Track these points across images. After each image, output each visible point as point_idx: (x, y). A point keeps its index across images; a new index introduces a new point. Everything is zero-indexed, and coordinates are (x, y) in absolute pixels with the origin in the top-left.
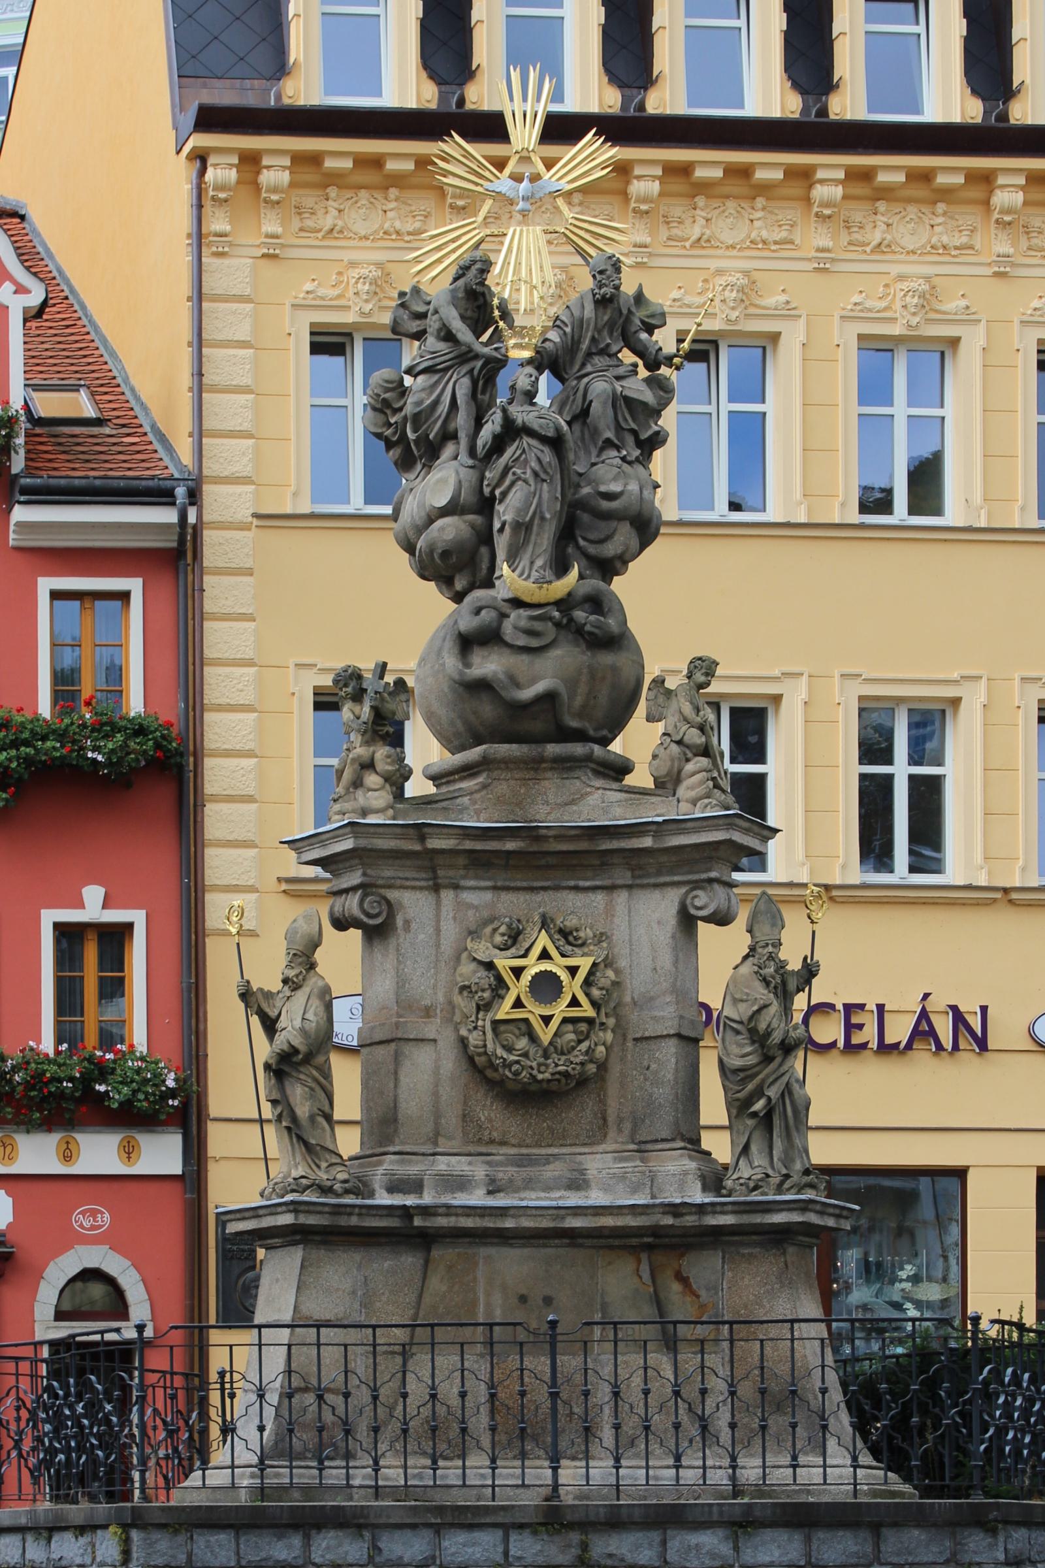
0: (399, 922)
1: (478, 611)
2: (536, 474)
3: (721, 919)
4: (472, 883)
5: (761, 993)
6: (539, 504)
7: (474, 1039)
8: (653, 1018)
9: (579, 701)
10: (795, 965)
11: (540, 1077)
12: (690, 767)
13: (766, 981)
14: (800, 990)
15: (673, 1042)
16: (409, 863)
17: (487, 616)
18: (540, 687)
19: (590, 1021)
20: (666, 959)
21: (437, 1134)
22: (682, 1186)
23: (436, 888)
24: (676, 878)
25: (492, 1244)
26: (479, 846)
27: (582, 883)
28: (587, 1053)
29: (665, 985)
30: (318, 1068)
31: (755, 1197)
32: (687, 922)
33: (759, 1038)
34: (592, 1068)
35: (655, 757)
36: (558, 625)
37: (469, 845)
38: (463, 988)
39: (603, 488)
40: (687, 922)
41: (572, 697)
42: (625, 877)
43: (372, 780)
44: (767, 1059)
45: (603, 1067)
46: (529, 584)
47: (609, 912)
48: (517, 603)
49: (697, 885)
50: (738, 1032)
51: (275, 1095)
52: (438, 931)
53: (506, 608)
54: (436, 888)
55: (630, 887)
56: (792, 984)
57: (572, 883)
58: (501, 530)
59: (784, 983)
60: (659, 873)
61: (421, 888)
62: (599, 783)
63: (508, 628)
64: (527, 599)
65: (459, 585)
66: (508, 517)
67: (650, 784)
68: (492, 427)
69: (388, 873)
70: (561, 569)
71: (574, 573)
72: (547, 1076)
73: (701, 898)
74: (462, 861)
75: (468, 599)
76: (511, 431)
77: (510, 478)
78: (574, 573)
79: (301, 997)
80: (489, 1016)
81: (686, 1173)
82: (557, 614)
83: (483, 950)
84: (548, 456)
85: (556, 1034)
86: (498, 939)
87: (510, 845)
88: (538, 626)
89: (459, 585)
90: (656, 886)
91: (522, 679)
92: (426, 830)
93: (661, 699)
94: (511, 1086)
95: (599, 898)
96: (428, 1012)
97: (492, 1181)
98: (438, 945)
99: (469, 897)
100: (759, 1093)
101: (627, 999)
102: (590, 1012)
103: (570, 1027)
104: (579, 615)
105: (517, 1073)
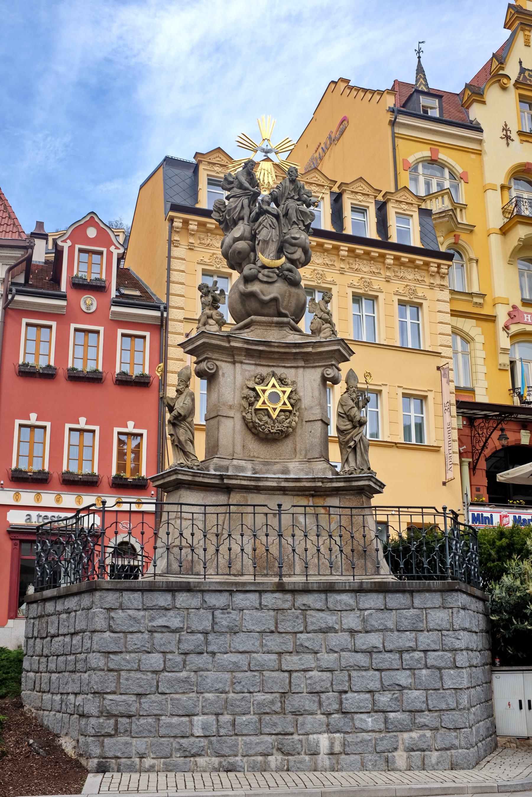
0: (220, 373)
1: (250, 269)
2: (271, 226)
6: (271, 236)
7: (248, 416)
8: (312, 414)
9: (285, 303)
11: (272, 431)
15: (320, 422)
18: (272, 296)
19: (290, 412)
20: (316, 393)
21: (234, 452)
22: (324, 473)
23: (234, 363)
24: (320, 364)
25: (254, 493)
27: (287, 365)
28: (289, 423)
29: (316, 402)
34: (290, 430)
35: (312, 323)
38: (244, 397)
39: (293, 236)
41: (283, 302)
43: (211, 321)
45: (294, 429)
46: (269, 260)
47: (296, 376)
48: (264, 267)
51: (172, 432)
52: (235, 378)
53: (260, 269)
55: (304, 367)
57: (283, 365)
58: (258, 244)
61: (229, 362)
62: (291, 332)
63: (260, 276)
64: (267, 265)
66: (261, 238)
67: (310, 333)
68: (256, 210)
70: (279, 258)
72: (274, 431)
74: (243, 353)
76: (262, 212)
77: (262, 226)
80: (253, 408)
81: (325, 468)
82: (278, 271)
83: (251, 384)
84: (274, 220)
85: (278, 416)
86: (257, 380)
87: (261, 348)
88: (271, 274)
90: (313, 367)
91: (265, 293)
93: (313, 306)
94: (261, 435)
95: (293, 371)
96: (231, 407)
97: (254, 469)
98: (235, 383)
101: (303, 407)
102: (290, 408)
103: (283, 413)
105: (263, 429)
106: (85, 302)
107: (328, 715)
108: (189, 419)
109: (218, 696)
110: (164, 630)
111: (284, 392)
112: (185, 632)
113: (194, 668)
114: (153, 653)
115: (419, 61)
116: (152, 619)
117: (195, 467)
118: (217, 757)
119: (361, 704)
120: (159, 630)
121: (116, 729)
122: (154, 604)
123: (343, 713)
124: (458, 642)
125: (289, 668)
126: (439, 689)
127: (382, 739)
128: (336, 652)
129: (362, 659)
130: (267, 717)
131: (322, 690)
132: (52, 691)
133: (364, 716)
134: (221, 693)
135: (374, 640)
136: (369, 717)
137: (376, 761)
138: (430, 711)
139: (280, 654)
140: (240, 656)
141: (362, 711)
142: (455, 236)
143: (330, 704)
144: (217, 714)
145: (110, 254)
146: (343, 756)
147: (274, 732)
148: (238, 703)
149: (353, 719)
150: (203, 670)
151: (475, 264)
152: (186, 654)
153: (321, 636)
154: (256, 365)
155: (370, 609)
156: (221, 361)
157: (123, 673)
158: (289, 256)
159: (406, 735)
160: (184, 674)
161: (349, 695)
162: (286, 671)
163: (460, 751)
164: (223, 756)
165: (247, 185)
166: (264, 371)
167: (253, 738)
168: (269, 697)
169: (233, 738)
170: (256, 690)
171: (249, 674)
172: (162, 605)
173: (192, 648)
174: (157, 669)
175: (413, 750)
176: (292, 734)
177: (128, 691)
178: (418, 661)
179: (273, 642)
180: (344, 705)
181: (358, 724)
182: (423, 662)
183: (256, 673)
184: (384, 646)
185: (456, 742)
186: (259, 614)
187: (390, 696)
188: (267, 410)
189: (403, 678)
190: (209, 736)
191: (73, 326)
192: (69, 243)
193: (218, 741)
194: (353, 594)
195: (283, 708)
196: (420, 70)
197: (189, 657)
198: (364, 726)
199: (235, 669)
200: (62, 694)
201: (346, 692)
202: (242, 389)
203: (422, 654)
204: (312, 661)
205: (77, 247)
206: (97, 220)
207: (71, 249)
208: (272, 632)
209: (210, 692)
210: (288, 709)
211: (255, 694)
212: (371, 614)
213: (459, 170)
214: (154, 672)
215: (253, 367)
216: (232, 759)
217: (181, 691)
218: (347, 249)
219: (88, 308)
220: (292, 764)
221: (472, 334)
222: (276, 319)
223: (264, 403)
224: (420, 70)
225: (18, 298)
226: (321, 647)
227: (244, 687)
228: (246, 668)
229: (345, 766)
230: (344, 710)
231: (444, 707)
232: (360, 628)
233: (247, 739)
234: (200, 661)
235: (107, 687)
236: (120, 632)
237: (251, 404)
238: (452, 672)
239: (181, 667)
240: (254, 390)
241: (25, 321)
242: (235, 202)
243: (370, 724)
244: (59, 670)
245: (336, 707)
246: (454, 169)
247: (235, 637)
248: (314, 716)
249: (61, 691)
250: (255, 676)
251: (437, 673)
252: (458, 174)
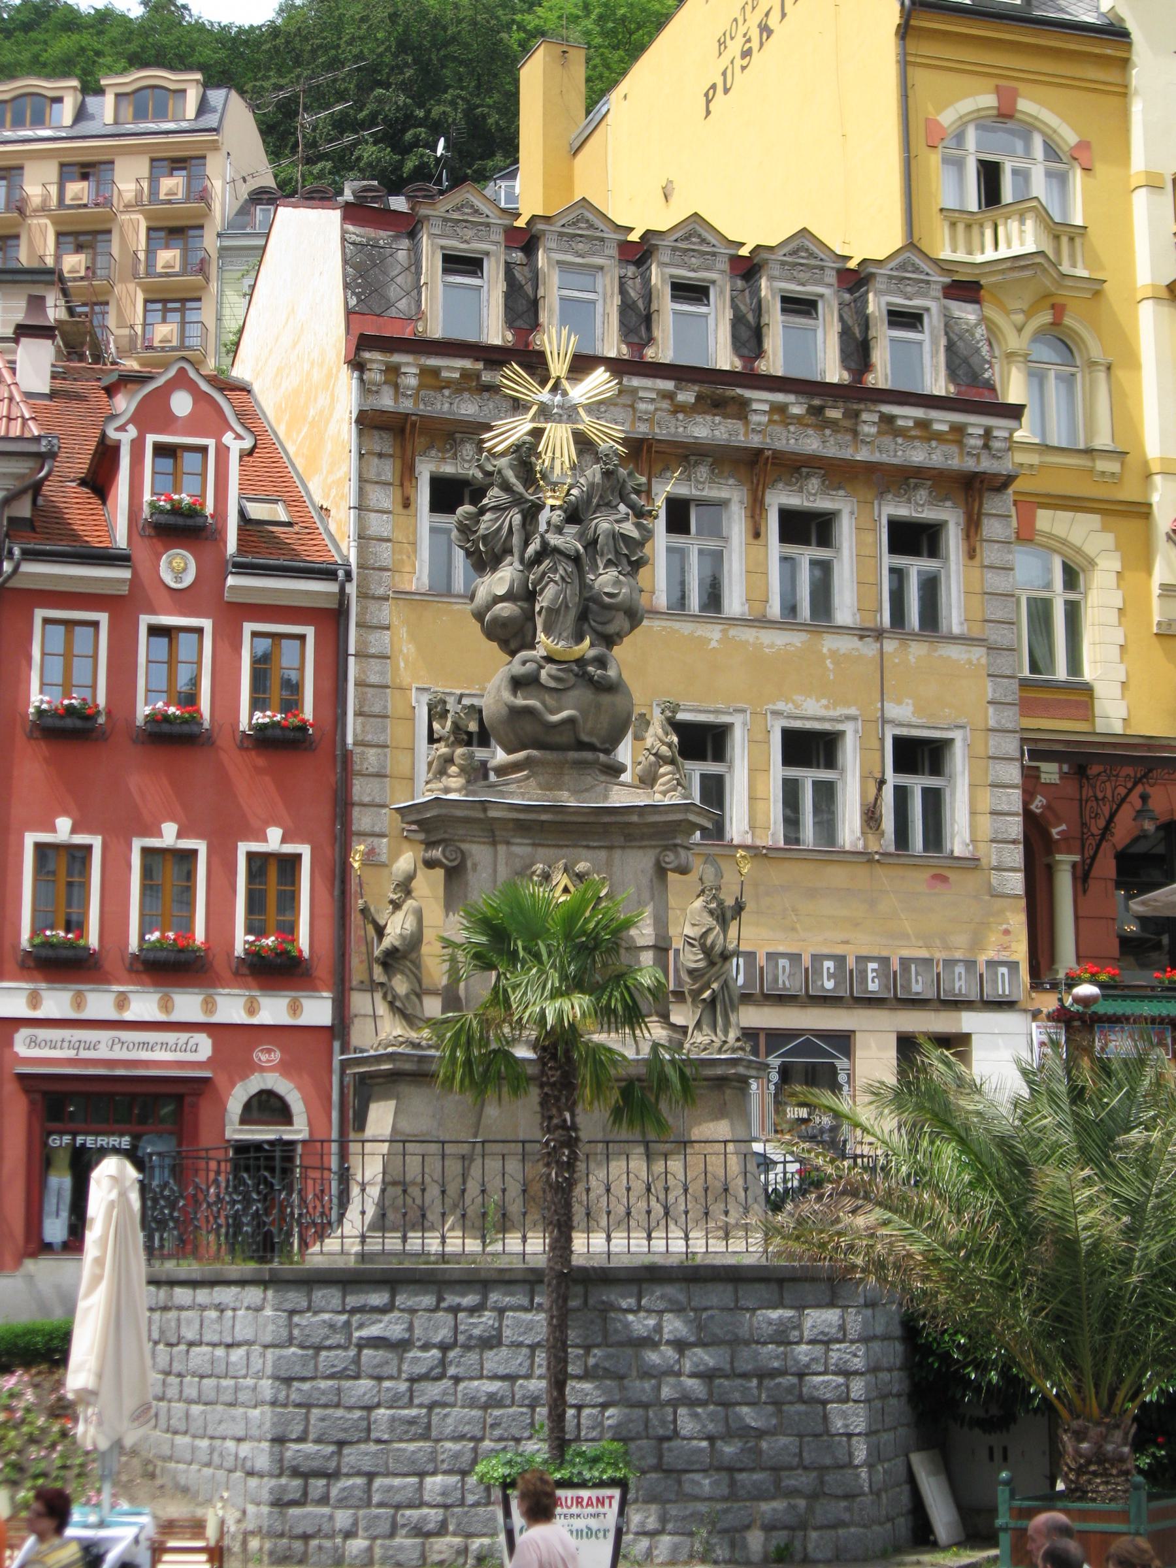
0: (469, 864)
1: (524, 663)
3: (683, 870)
4: (518, 840)
5: (710, 921)
10: (730, 902)
12: (662, 770)
13: (711, 912)
14: (733, 918)
17: (531, 666)
23: (494, 843)
26: (522, 816)
30: (412, 962)
31: (704, 1055)
32: (661, 872)
33: (707, 951)
36: (576, 675)
37: (515, 815)
40: (661, 872)
42: (620, 840)
43: (453, 770)
44: (712, 964)
49: (666, 848)
50: (693, 946)
52: (495, 871)
53: (543, 663)
54: (494, 843)
55: (623, 848)
56: (729, 914)
59: (723, 915)
60: (642, 839)
65: (513, 646)
69: (461, 832)
70: (579, 639)
71: (587, 641)
73: (670, 857)
75: (519, 656)
78: (587, 641)
79: (400, 915)
82: (576, 668)
87: (544, 817)
89: (513, 646)
98: (495, 882)
99: (517, 850)
100: (707, 986)
104: (591, 669)
106: (170, 563)
108: (413, 956)
113: (427, 1402)
116: (361, 1326)
117: (424, 1043)
119: (694, 1458)
121: (305, 1493)
123: (665, 1471)
124: (856, 1360)
126: (821, 1435)
127: (726, 1511)
128: (654, 1377)
131: (633, 1434)
132: (192, 1431)
133: (697, 1477)
138: (805, 1468)
142: (1053, 306)
143: (643, 1458)
145: (222, 452)
149: (679, 1482)
151: (1102, 376)
153: (629, 1351)
154: (534, 845)
155: (711, 1308)
158: (599, 628)
159: (765, 1507)
160: (414, 1412)
163: (852, 1530)
165: (519, 488)
173: (424, 1370)
178: (790, 1389)
180: (665, 1459)
181: (687, 1488)
182: (796, 1392)
184: (733, 1368)
185: (846, 1517)
186: (528, 1316)
187: (740, 1444)
191: (145, 620)
192: (132, 432)
194: (684, 1285)
198: (696, 1491)
199: (494, 1401)
200: (212, 1438)
201: (669, 1439)
203: (794, 1380)
204: (616, 1391)
205: (151, 439)
206: (192, 374)
207: (137, 446)
212: (712, 1317)
213: (1069, 137)
215: (529, 849)
218: (766, 407)
219: (178, 579)
221: (1090, 549)
222: (573, 755)
225: (28, 568)
226: (630, 1369)
228: (508, 1402)
231: (828, 1461)
232: (692, 1339)
239: (406, 1399)
241: (40, 614)
242: (497, 519)
243: (707, 1488)
244: (204, 1398)
245: (652, 1461)
246: (1055, 136)
249: (210, 1432)
252: (1066, 149)
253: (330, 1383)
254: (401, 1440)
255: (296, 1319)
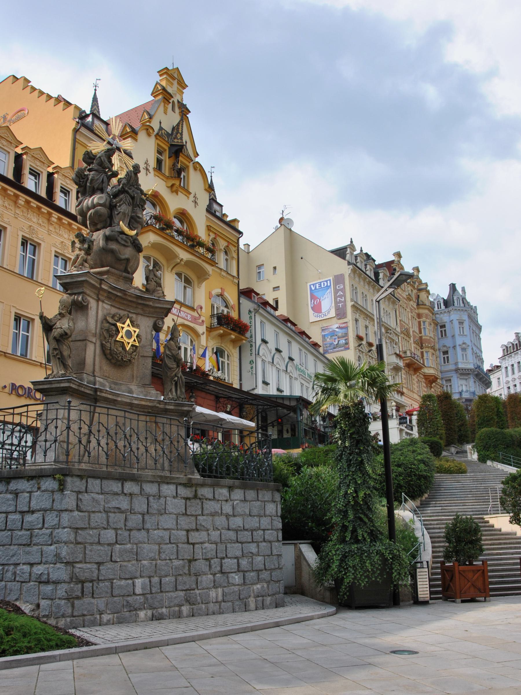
16: (94, 290)
87: (119, 294)
92: (103, 282)
107: (214, 575)
109: (151, 563)
110: (116, 510)
111: (135, 332)
112: (129, 513)
113: (136, 541)
114: (108, 529)
115: (95, 93)
118: (151, 609)
119: (233, 567)
120: (113, 511)
122: (110, 489)
125: (193, 541)
127: (243, 590)
129: (232, 535)
130: (180, 578)
133: (233, 575)
134: (153, 560)
135: (237, 522)
136: (236, 575)
137: (240, 605)
139: (188, 531)
140: (165, 532)
141: (233, 571)
144: (150, 577)
146: (223, 604)
147: (184, 589)
148: (163, 568)
149: (228, 577)
150: (141, 543)
152: (130, 530)
154: (111, 305)
156: (91, 297)
157: (88, 546)
161: (226, 560)
162: (192, 544)
164: (155, 608)
166: (122, 313)
167: (172, 594)
168: (181, 562)
169: (160, 594)
170: (174, 558)
171: (170, 546)
172: (115, 491)
173: (135, 525)
174: (112, 542)
175: (258, 596)
176: (194, 590)
177: (91, 560)
179: (184, 522)
183: (174, 545)
188: (123, 342)
189: (253, 548)
190: (145, 594)
193: (151, 597)
195: (189, 570)
196: (95, 99)
197: (133, 533)
201: (224, 558)
202: (102, 322)
208: (183, 514)
209: (146, 560)
210: (193, 571)
211: (173, 561)
214: (109, 545)
215: (109, 307)
216: (160, 611)
217: (127, 560)
220: (195, 611)
223: (122, 337)
224: (95, 99)
227: (167, 555)
228: (168, 542)
229: (224, 610)
230: (223, 571)
231: (273, 567)
233: (169, 594)
234: (140, 536)
235: (76, 557)
236: (85, 512)
237: (111, 336)
238: (276, 544)
239: (128, 540)
240: (115, 325)
247: (161, 518)
248: (206, 576)
250: (173, 547)
251: (269, 545)
253: (95, 531)
254: (125, 561)
255: (80, 496)
